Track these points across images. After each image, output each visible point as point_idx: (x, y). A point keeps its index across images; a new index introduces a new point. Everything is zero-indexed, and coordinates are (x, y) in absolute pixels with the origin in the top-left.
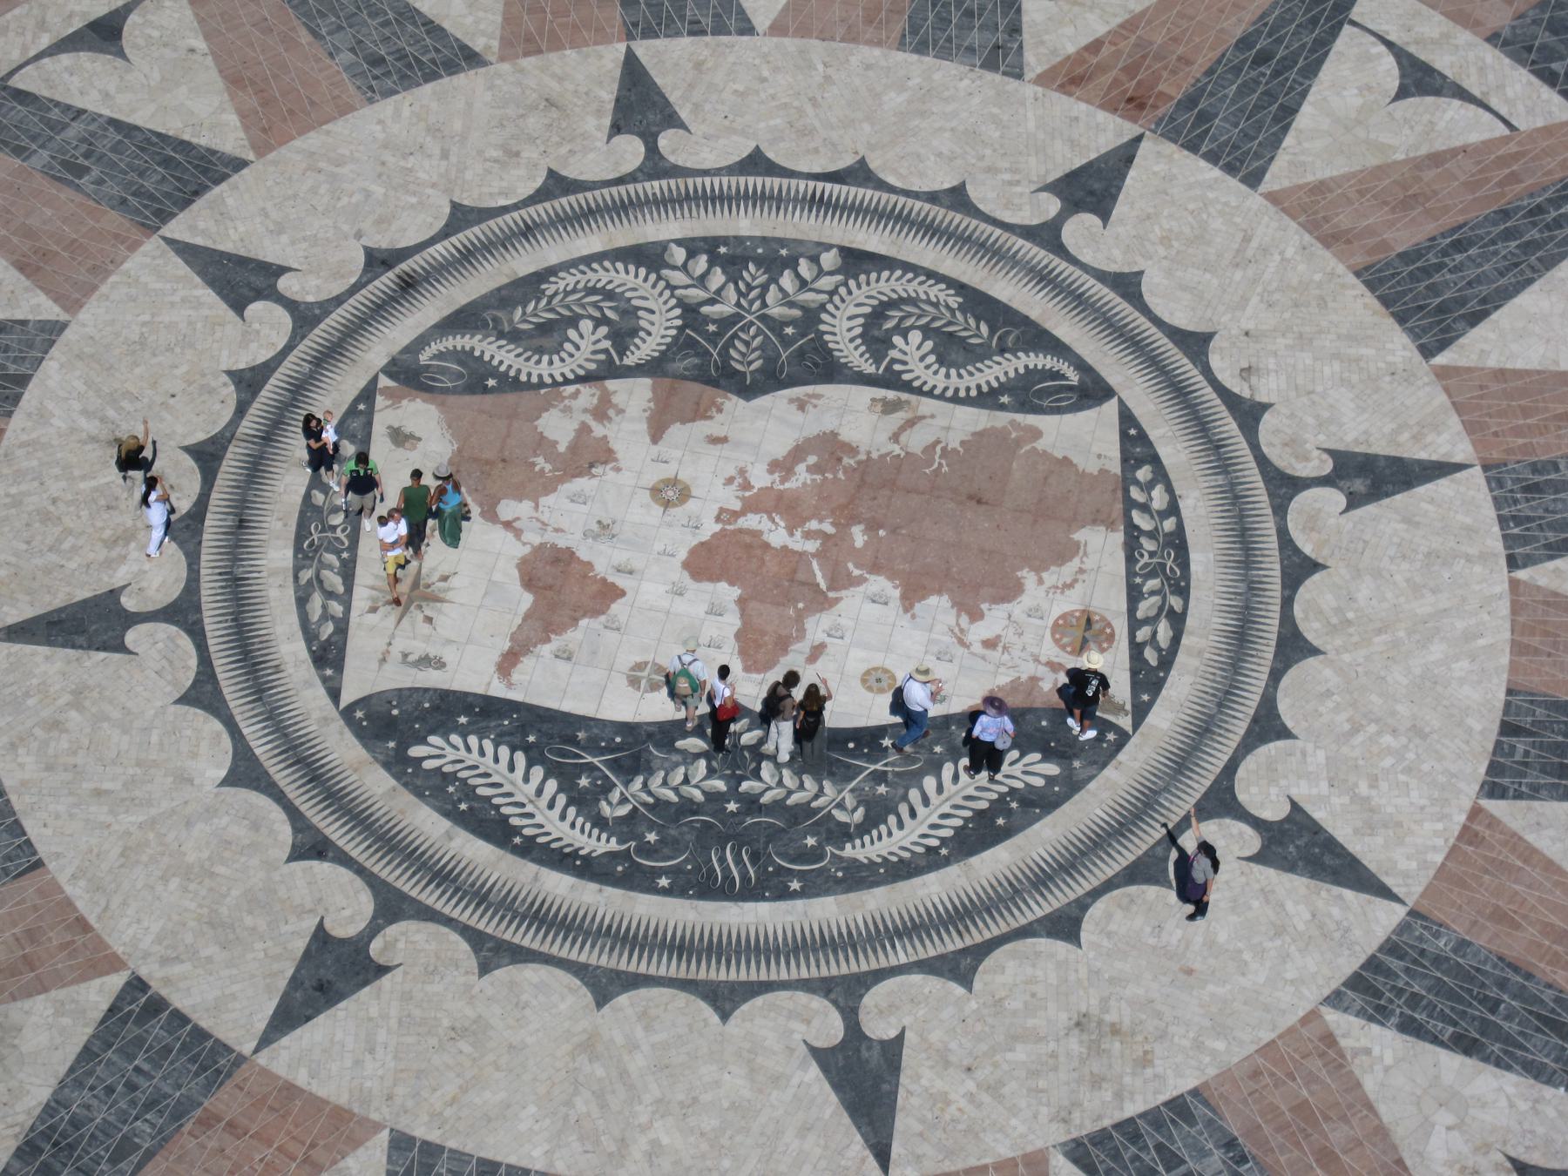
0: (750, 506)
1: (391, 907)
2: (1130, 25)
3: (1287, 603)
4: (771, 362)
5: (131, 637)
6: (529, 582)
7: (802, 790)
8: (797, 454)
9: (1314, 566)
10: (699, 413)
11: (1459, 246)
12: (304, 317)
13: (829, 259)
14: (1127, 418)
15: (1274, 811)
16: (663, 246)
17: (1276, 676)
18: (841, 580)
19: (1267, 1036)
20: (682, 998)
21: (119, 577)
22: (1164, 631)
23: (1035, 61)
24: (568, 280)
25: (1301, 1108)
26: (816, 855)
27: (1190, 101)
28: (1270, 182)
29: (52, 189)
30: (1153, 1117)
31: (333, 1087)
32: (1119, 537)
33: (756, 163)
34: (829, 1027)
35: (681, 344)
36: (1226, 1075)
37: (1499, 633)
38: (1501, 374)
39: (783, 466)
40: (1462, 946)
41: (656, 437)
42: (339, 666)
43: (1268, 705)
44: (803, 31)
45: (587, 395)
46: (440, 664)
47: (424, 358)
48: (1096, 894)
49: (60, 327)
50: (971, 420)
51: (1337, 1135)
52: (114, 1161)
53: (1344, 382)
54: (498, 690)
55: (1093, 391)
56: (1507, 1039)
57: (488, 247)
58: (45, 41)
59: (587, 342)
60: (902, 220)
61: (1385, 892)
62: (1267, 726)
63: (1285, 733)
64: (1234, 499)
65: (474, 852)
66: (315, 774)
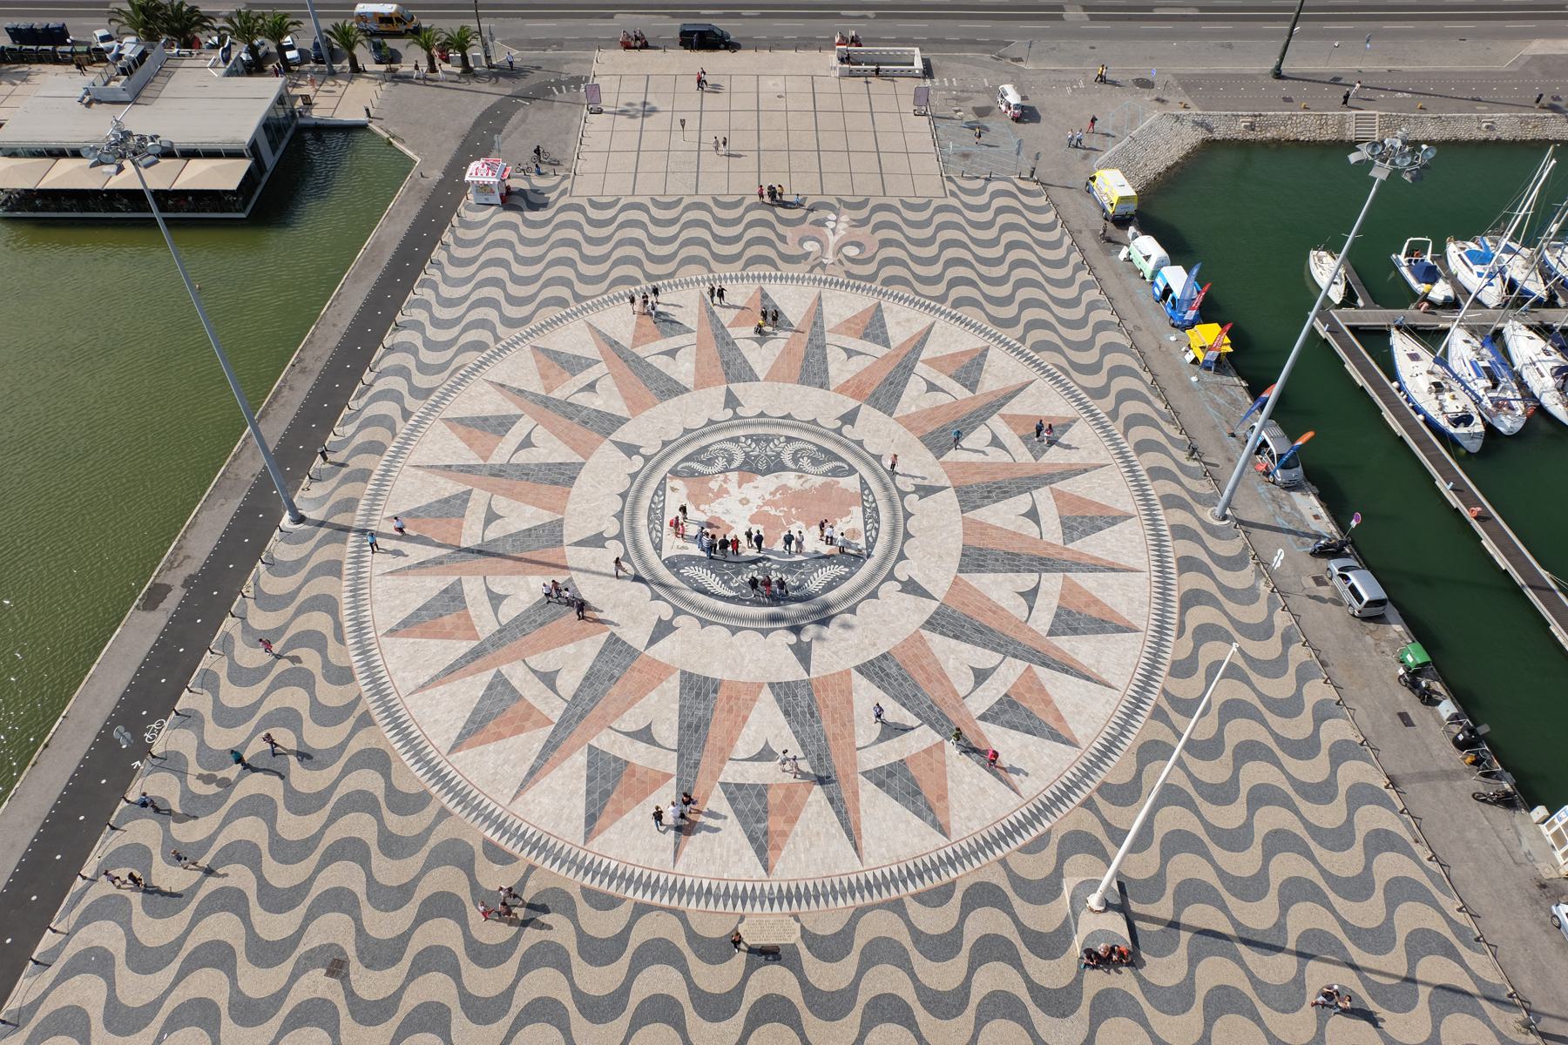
0: (766, 504)
1: (678, 612)
2: (857, 375)
4: (769, 466)
8: (777, 490)
10: (750, 480)
11: (944, 430)
12: (647, 459)
13: (782, 439)
14: (861, 478)
15: (905, 579)
17: (903, 543)
18: (790, 522)
22: (874, 533)
23: (832, 388)
24: (715, 447)
25: (915, 655)
27: (874, 394)
28: (894, 416)
29: (580, 428)
30: (876, 658)
33: (762, 415)
35: (745, 463)
36: (895, 648)
37: (959, 529)
38: (957, 463)
39: (773, 494)
40: (954, 611)
43: (901, 551)
44: (772, 380)
45: (722, 477)
50: (820, 480)
51: (925, 662)
57: (693, 439)
59: (721, 463)
62: (902, 557)
64: (890, 500)
65: (700, 598)
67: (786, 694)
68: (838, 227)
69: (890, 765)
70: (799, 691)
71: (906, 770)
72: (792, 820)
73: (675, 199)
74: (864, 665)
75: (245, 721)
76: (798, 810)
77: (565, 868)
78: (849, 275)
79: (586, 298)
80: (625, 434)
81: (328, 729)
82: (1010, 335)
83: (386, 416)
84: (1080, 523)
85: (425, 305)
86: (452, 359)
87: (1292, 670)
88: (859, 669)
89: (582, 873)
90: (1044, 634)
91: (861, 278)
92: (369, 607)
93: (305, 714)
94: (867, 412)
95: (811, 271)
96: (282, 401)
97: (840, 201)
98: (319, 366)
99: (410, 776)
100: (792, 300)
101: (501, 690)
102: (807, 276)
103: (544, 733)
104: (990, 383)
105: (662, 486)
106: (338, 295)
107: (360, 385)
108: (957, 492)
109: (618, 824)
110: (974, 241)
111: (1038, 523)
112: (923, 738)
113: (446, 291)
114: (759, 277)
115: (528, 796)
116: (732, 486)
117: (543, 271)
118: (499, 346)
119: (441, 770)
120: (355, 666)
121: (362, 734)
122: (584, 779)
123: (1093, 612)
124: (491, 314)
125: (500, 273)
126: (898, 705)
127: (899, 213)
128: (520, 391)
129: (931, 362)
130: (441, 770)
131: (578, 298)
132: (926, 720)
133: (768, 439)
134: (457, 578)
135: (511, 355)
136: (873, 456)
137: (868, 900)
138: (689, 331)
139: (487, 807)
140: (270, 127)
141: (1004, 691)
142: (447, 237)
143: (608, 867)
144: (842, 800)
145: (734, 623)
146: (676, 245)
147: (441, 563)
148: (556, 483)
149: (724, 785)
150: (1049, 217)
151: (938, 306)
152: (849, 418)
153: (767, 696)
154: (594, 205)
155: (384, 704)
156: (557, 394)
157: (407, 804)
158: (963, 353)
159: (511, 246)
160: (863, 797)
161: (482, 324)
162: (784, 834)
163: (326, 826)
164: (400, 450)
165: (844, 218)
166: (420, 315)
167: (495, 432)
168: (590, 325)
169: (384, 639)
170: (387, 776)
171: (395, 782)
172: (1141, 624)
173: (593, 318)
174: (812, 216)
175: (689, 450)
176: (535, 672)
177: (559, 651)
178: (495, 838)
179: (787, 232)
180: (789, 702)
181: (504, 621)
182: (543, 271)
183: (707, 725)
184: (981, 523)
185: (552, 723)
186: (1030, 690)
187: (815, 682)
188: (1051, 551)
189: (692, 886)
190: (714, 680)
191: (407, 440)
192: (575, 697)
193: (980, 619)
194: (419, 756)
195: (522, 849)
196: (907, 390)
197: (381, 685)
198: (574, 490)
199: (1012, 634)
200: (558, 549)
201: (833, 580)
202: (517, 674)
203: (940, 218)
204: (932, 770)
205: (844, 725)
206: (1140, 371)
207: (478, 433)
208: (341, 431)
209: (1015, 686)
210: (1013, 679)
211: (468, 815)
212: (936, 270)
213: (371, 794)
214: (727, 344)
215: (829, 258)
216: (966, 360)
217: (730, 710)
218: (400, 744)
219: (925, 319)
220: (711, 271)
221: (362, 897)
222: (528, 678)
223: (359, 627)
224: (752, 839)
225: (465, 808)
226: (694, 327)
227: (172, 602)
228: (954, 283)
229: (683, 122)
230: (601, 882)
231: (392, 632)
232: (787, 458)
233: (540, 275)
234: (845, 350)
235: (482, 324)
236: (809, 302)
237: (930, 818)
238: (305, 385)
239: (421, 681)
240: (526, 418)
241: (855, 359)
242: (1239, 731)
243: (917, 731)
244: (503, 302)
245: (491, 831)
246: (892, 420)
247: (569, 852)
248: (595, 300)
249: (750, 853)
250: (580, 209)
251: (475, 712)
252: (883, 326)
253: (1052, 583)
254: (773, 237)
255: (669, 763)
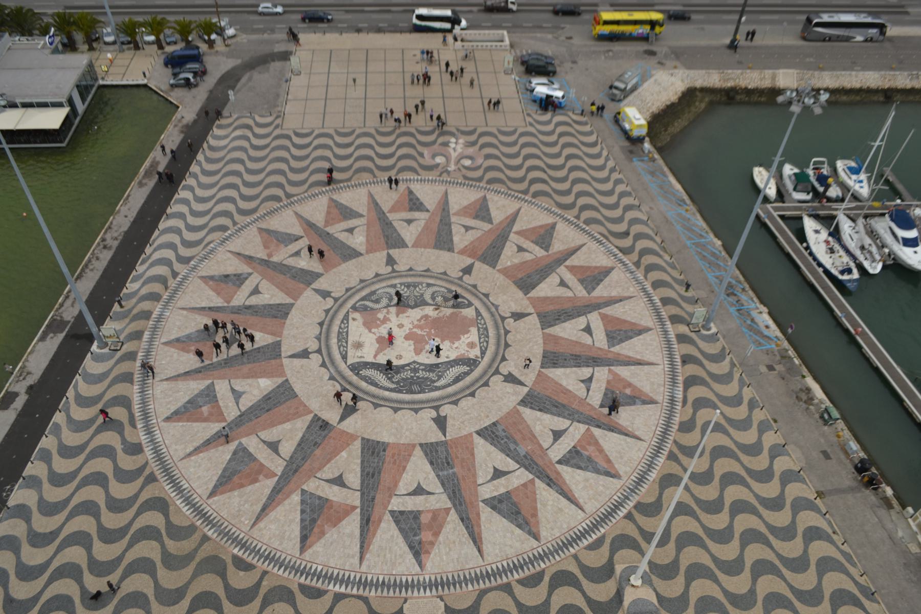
0: (414, 327)
2: (472, 242)
3: (505, 338)
5: (310, 356)
6: (378, 342)
7: (427, 375)
8: (422, 318)
9: (509, 332)
10: (404, 312)
12: (336, 300)
13: (424, 285)
14: (476, 309)
15: (506, 373)
16: (396, 285)
17: (504, 350)
19: (508, 411)
20: (409, 411)
21: (308, 346)
22: (485, 344)
23: (456, 251)
24: (380, 291)
26: (430, 385)
27: (483, 255)
28: (497, 268)
30: (490, 426)
31: (350, 431)
32: (476, 329)
33: (411, 269)
34: (434, 414)
36: (501, 418)
37: (541, 341)
38: (538, 298)
39: (419, 320)
40: (539, 393)
41: (397, 316)
42: (346, 359)
44: (417, 247)
45: (385, 310)
46: (363, 357)
47: (357, 305)
48: (477, 389)
49: (292, 305)
50: (451, 311)
52: (314, 445)
53: (512, 300)
54: (374, 361)
55: (470, 304)
56: (548, 409)
58: (288, 255)
59: (384, 301)
60: (436, 278)
61: (526, 386)
62: (504, 359)
63: (506, 360)
65: (372, 389)
66: (344, 378)
67: (431, 450)
68: (457, 147)
69: (500, 495)
70: (439, 448)
71: (510, 498)
72: (437, 534)
73: (350, 130)
74: (481, 430)
75: (70, 482)
76: (441, 527)
77: (287, 572)
78: (465, 178)
79: (294, 195)
80: (322, 284)
81: (126, 485)
82: (570, 215)
83: (160, 276)
84: (619, 334)
85: (185, 202)
86: (205, 237)
87: (755, 426)
88: (479, 433)
89: (299, 574)
90: (597, 407)
91: (472, 179)
92: (152, 403)
93: (110, 475)
94: (478, 265)
95: (440, 176)
96: (91, 267)
97: (458, 130)
98: (116, 244)
99: (183, 513)
100: (428, 194)
101: (242, 454)
102: (438, 179)
103: (271, 483)
104: (557, 246)
105: (346, 317)
106: (129, 196)
107: (143, 256)
108: (538, 316)
109: (323, 541)
110: (546, 154)
111: (591, 334)
112: (521, 476)
113: (200, 192)
114: (407, 180)
115: (261, 525)
116: (393, 317)
117: (264, 178)
118: (236, 228)
119: (203, 510)
120: (143, 442)
121: (149, 487)
122: (299, 512)
123: (628, 391)
124: (230, 207)
125: (236, 180)
126: (504, 456)
127: (496, 137)
128: (250, 258)
129: (517, 233)
130: (203, 510)
131: (288, 196)
132: (522, 465)
133: (415, 286)
134: (210, 381)
135: (244, 233)
136: (483, 294)
137: (488, 584)
138: (361, 216)
139: (234, 533)
140: (83, 90)
141: (573, 444)
142: (200, 157)
143: (316, 570)
144: (468, 519)
145: (395, 405)
146: (352, 160)
147: (200, 372)
148: (276, 317)
149: (392, 513)
150: (592, 139)
151: (523, 196)
152: (468, 270)
153: (418, 452)
154: (297, 135)
155: (163, 467)
156: (275, 259)
157: (179, 532)
158: (541, 227)
159: (241, 161)
160: (483, 517)
161: (226, 214)
162: (432, 544)
163: (126, 550)
164: (171, 298)
165: (461, 141)
166: (184, 209)
167: (234, 284)
168: (296, 214)
169: (163, 424)
170: (166, 515)
171: (172, 519)
172: (659, 398)
173: (299, 208)
174: (441, 140)
175: (364, 293)
176: (264, 442)
177: (280, 427)
178: (240, 554)
179: (426, 152)
180: (433, 455)
181: (243, 409)
182: (264, 178)
183: (379, 473)
184: (554, 336)
185: (277, 475)
186: (589, 444)
187: (449, 442)
188: (600, 353)
189: (372, 580)
190: (383, 443)
191: (175, 291)
192: (291, 457)
193: (556, 398)
194: (188, 501)
195: (258, 561)
196: (504, 252)
197: (161, 454)
198: (288, 322)
199: (577, 408)
200: (278, 361)
201: (460, 375)
202: (252, 443)
203: (523, 140)
204: (528, 498)
205: (469, 470)
206: (653, 235)
207: (223, 285)
208: (131, 286)
209: (579, 441)
210: (578, 437)
211: (222, 539)
212: (520, 174)
213: (156, 527)
214: (387, 224)
215: (452, 168)
216: (542, 232)
217: (394, 463)
218: (174, 494)
219: (516, 205)
220: (375, 176)
221: (152, 598)
222: (260, 446)
223: (146, 416)
224: (411, 547)
225: (219, 534)
226: (365, 213)
227: (19, 403)
228: (533, 181)
229: (354, 80)
230: (312, 580)
231: (168, 419)
232: (427, 297)
233: (262, 181)
234: (464, 226)
235: (226, 214)
236: (440, 196)
237: (527, 529)
238: (106, 256)
239: (188, 451)
240: (255, 275)
241: (470, 232)
242: (724, 466)
243: (517, 473)
244: (238, 199)
245: (237, 549)
246: (495, 271)
247: (290, 561)
248: (299, 197)
249: (410, 556)
250: (288, 137)
251: (225, 470)
252: (488, 210)
253: (602, 375)
254: (416, 154)
255: (355, 499)
